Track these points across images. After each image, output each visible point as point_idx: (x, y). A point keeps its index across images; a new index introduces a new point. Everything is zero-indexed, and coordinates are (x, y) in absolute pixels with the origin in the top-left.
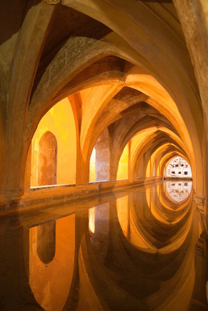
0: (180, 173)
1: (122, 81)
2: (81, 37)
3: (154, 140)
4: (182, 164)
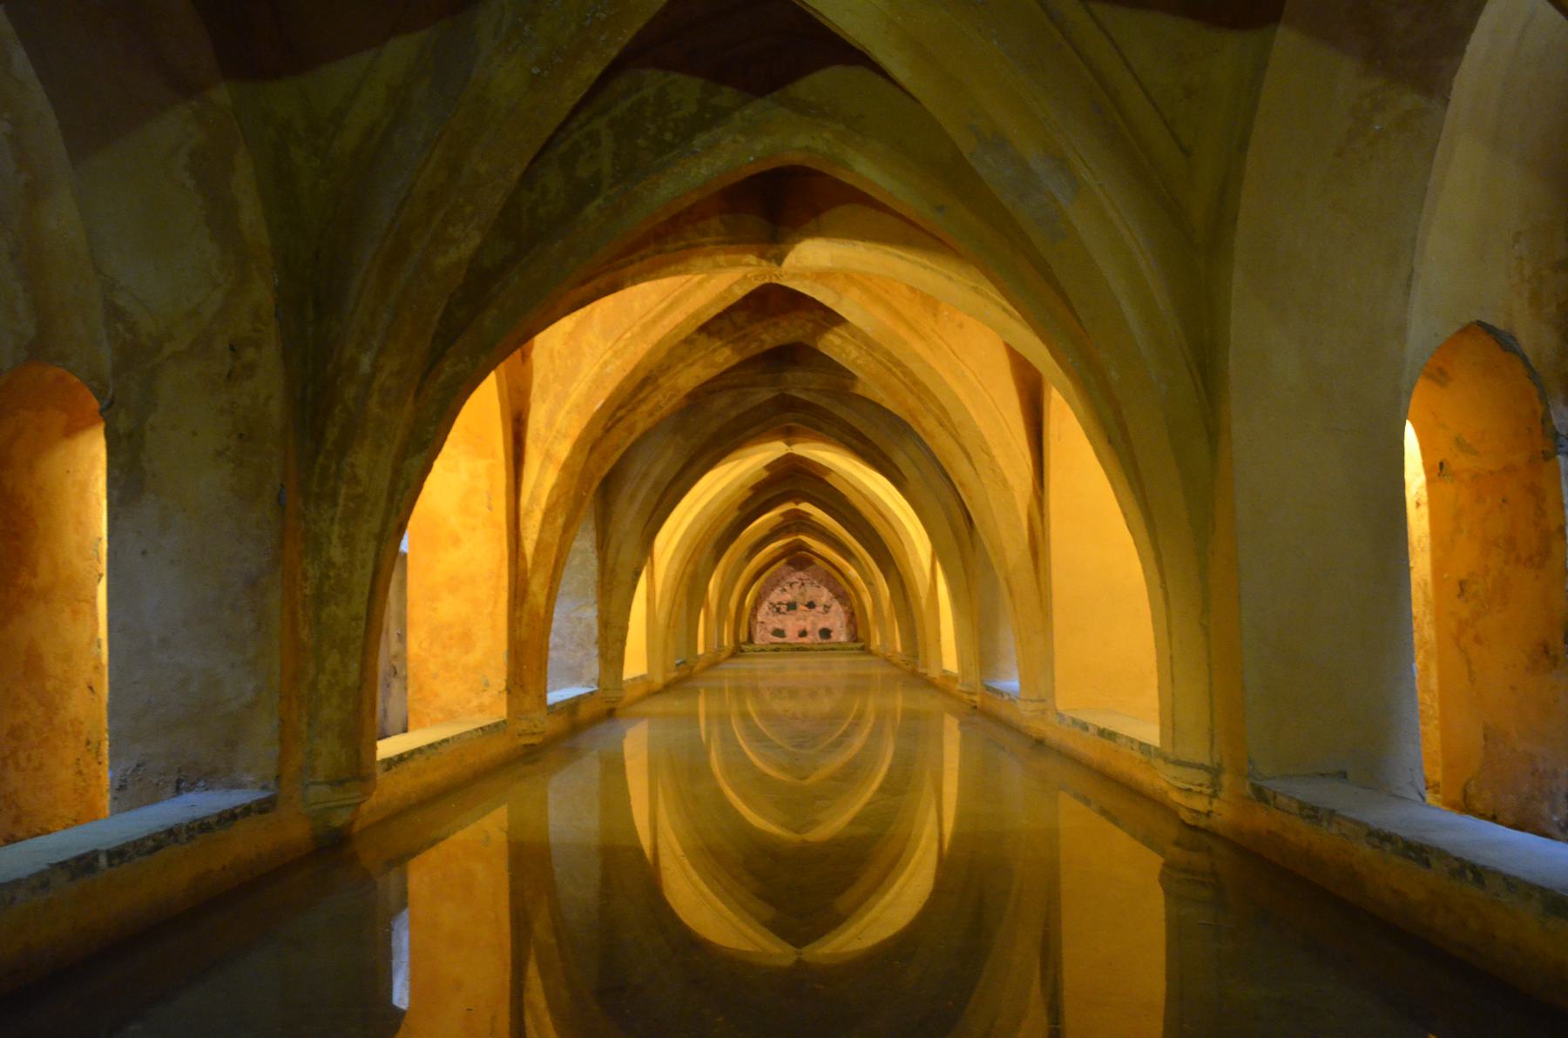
1: (769, 260)
2: (674, 76)
3: (750, 494)
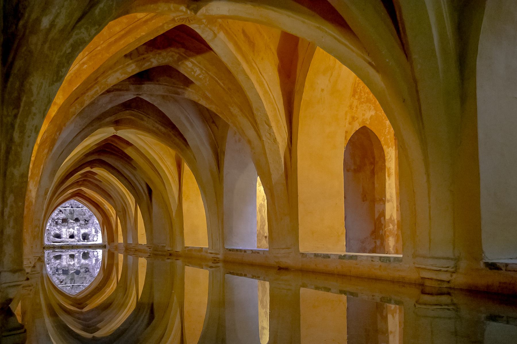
0: (72, 236)
4: (75, 217)
